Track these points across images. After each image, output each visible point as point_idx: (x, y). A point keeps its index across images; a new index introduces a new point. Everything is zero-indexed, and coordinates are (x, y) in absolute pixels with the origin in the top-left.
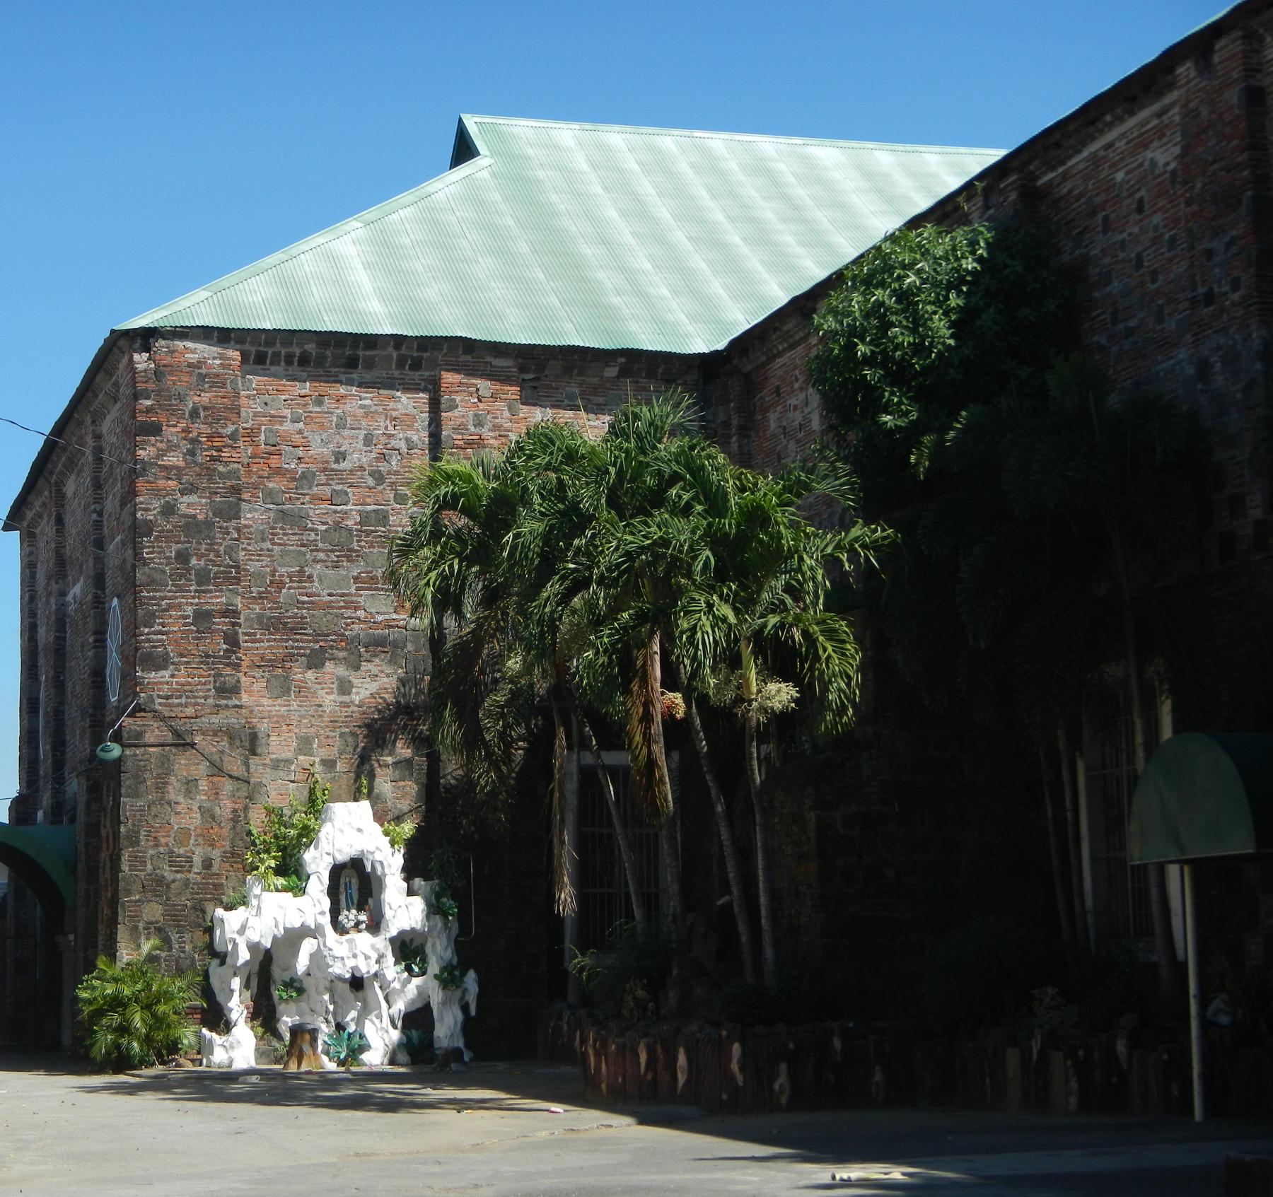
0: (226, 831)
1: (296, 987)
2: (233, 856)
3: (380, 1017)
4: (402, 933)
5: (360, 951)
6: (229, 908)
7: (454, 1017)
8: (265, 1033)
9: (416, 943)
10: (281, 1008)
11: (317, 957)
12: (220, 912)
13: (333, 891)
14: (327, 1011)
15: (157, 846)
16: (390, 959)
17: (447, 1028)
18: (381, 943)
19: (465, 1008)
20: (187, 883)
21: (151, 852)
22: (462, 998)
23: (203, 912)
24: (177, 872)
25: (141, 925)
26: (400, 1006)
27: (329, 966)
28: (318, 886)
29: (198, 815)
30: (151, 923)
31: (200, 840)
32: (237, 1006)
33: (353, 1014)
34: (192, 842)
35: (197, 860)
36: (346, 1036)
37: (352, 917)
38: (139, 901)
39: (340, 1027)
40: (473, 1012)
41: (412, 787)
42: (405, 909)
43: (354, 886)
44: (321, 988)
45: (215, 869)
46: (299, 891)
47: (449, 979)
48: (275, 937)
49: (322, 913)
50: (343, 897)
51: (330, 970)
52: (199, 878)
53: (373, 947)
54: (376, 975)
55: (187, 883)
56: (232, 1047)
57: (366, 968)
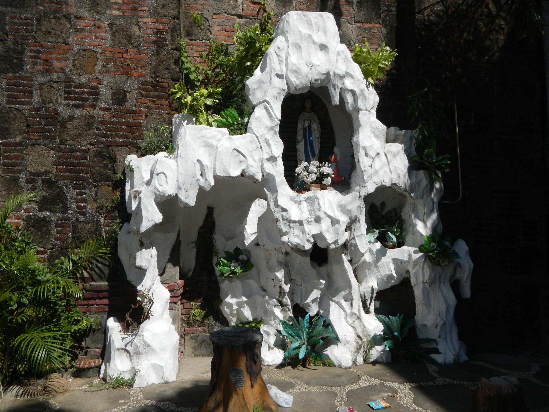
0: (145, 57)
1: (242, 258)
2: (156, 89)
3: (349, 299)
4: (381, 190)
5: (321, 214)
6: (142, 154)
7: (446, 300)
8: (205, 317)
9: (388, 208)
10: (224, 285)
11: (267, 221)
12: (132, 159)
13: (287, 130)
14: (282, 293)
15: (48, 71)
16: (363, 226)
17: (432, 312)
18: (353, 202)
19: (456, 286)
20: (90, 121)
21: (40, 79)
22: (453, 276)
23: (113, 160)
24: (76, 106)
25: (23, 177)
26: (372, 283)
27: (283, 234)
28: (265, 121)
29: (108, 35)
30: (38, 174)
31: (110, 66)
32: (156, 289)
33: (316, 294)
34: (98, 68)
35: (105, 92)
36: (305, 322)
37: (313, 168)
38: (20, 144)
39: (299, 311)
40: (467, 292)
41: (379, 29)
42: (382, 158)
43: (314, 126)
44: (274, 262)
45: (130, 104)
46: (239, 128)
47: (437, 252)
48: (201, 190)
49: (272, 159)
50: (301, 147)
51: (285, 239)
52: (107, 116)
53: (343, 209)
54: (345, 246)
55: (90, 121)
56: (138, 353)
57: (333, 236)
